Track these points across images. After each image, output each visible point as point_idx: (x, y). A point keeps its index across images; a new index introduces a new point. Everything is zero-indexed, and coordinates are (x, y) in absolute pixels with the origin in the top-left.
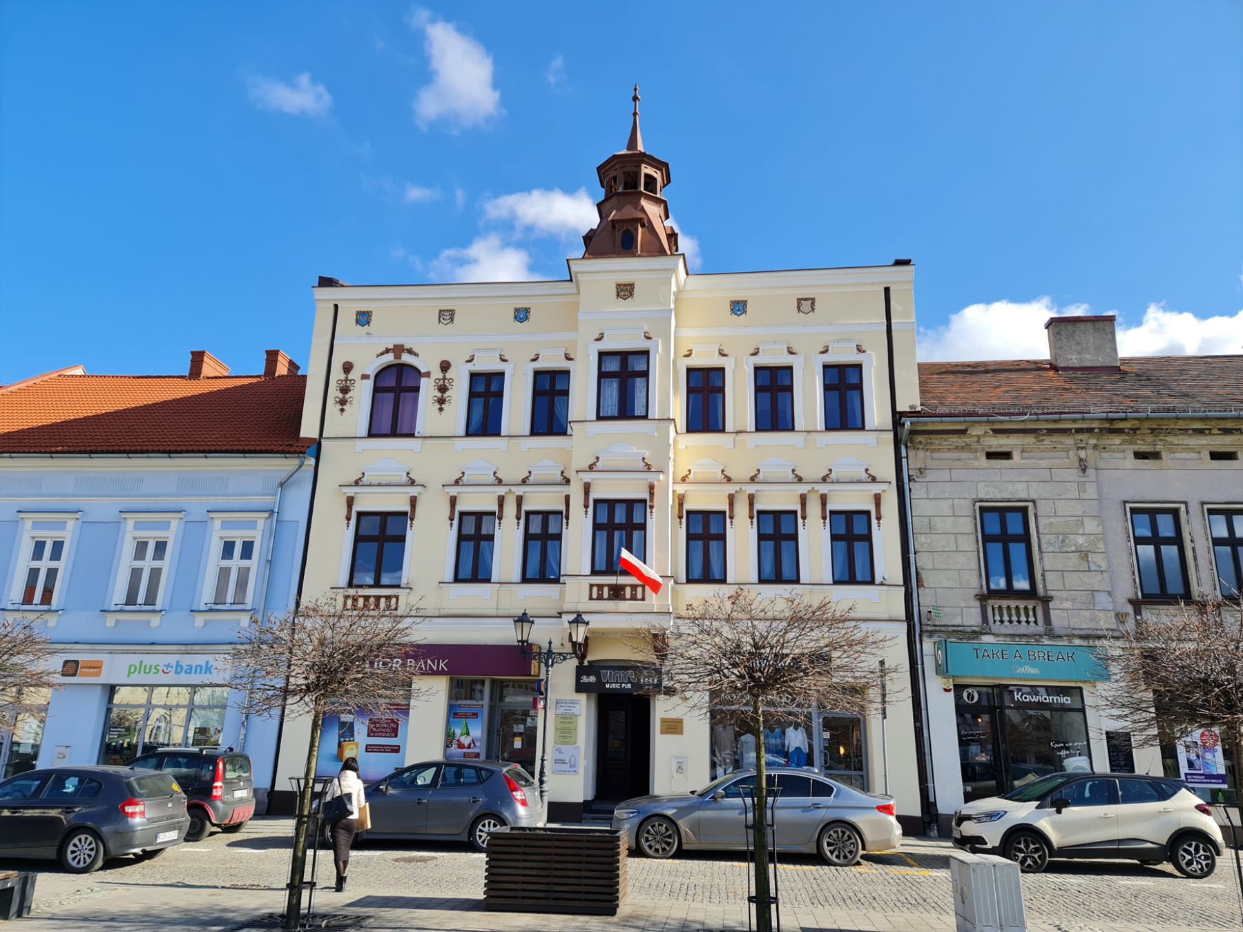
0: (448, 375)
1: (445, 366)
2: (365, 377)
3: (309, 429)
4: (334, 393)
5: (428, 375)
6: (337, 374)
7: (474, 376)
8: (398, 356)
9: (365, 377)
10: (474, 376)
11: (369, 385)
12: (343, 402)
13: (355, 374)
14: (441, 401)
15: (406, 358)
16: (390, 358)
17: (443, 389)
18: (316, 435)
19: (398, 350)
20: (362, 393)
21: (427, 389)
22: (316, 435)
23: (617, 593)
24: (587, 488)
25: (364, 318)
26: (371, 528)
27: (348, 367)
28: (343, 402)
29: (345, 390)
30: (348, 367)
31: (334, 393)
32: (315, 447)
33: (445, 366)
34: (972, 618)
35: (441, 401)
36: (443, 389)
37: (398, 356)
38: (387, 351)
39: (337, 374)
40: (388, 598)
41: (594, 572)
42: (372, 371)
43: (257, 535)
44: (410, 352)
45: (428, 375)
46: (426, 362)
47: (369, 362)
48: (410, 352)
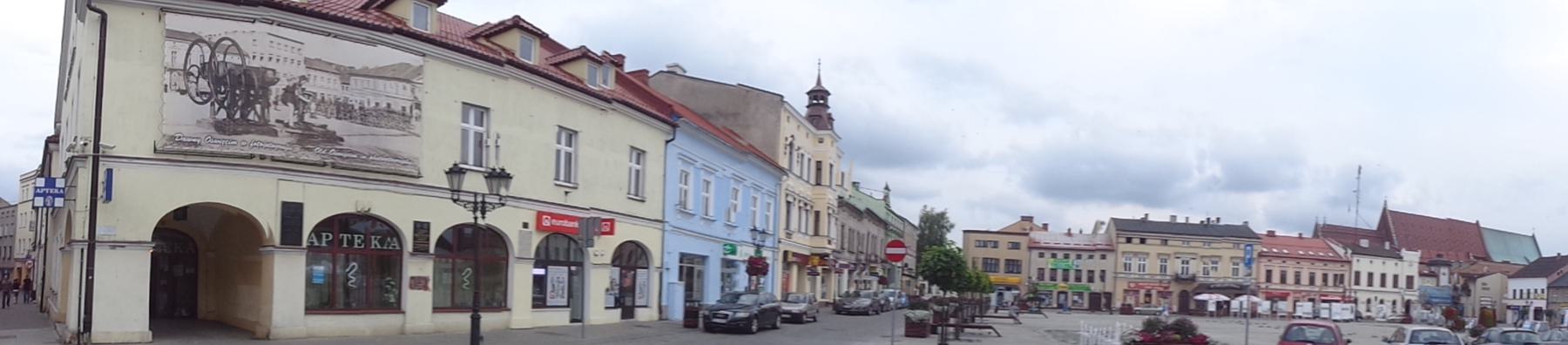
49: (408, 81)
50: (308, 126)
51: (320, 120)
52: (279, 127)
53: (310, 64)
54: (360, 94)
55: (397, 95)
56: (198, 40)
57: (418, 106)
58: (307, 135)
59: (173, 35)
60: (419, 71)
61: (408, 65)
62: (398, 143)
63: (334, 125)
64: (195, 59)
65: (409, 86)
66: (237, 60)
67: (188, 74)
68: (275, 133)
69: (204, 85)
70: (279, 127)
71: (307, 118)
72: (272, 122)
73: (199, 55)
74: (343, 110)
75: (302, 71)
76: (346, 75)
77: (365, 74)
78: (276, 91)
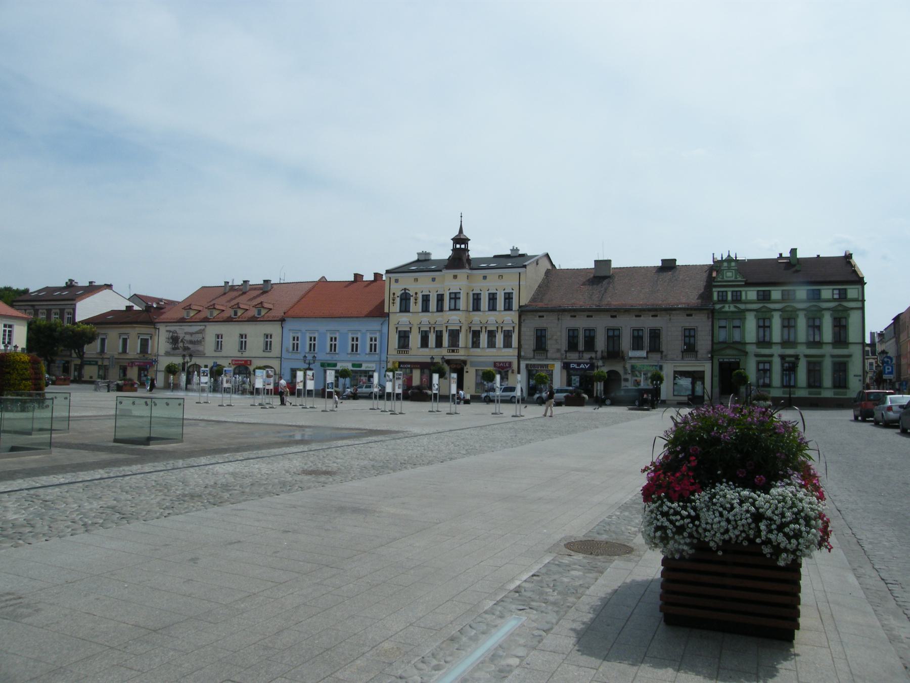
0: (417, 296)
1: (416, 294)
2: (398, 297)
3: (386, 310)
4: (391, 301)
5: (412, 296)
6: (392, 296)
7: (423, 296)
8: (405, 291)
9: (398, 297)
10: (423, 296)
11: (399, 299)
12: (393, 303)
13: (396, 296)
14: (416, 303)
15: (407, 291)
16: (403, 291)
17: (416, 300)
18: (388, 312)
19: (405, 289)
20: (398, 300)
21: (412, 300)
22: (388, 312)
23: (453, 351)
24: (447, 327)
25: (397, 281)
26: (402, 335)
27: (394, 294)
28: (393, 303)
29: (394, 300)
30: (394, 294)
31: (391, 301)
32: (388, 315)
33: (416, 294)
34: (532, 355)
35: (416, 303)
36: (416, 300)
37: (405, 291)
38: (403, 290)
39: (392, 296)
40: (407, 351)
41: (448, 347)
42: (399, 295)
43: (378, 336)
44: (408, 290)
45: (412, 296)
46: (412, 293)
47: (399, 293)
48: (408, 290)
49: (201, 333)
51: (187, 345)
53: (186, 333)
55: (198, 337)
57: (203, 338)
59: (167, 331)
60: (204, 330)
62: (200, 348)
63: (190, 346)
64: (170, 336)
66: (176, 335)
69: (171, 341)
71: (185, 345)
72: (179, 346)
73: (171, 334)
74: (191, 342)
75: (184, 335)
76: (191, 334)
78: (180, 340)
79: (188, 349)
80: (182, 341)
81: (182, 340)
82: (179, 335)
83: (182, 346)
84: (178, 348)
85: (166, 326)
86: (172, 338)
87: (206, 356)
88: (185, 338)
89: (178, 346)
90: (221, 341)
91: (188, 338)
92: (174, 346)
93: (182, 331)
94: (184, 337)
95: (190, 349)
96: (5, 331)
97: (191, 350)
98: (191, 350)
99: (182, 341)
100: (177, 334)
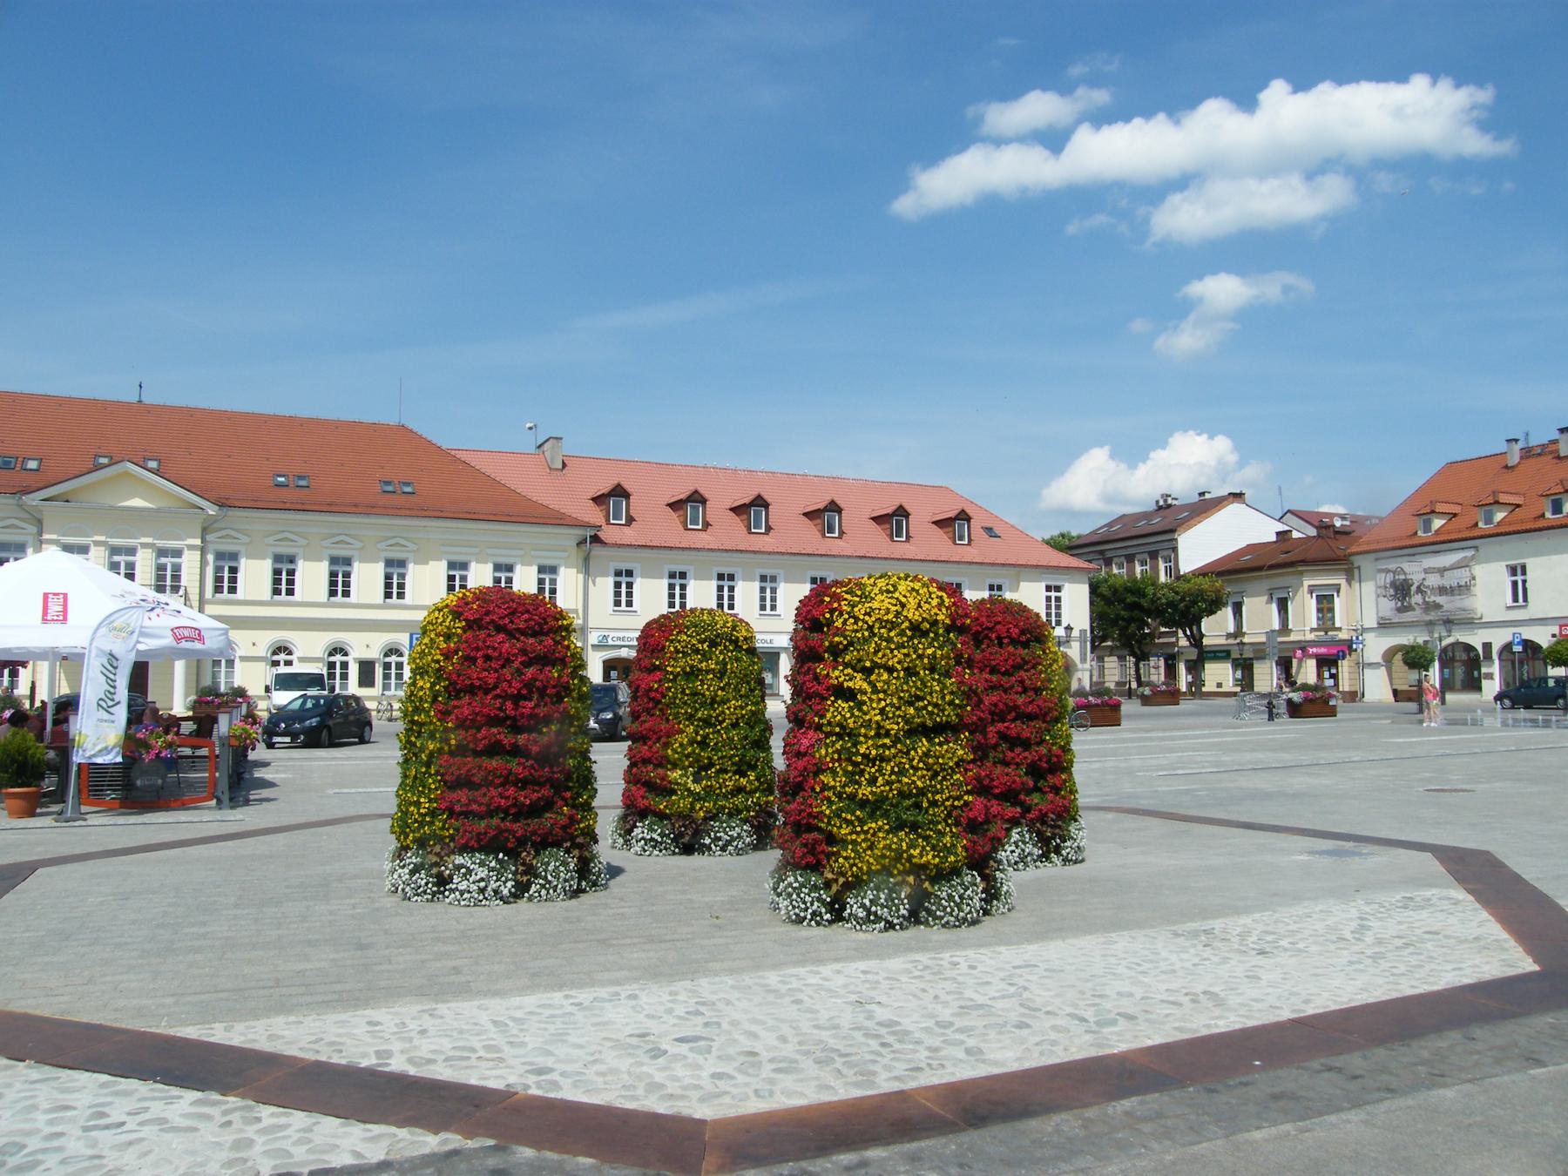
49: (1467, 566)
50: (1427, 603)
52: (1416, 606)
53: (1426, 571)
54: (1450, 580)
55: (1460, 576)
56: (1388, 571)
57: (1474, 578)
58: (1430, 607)
61: (1466, 557)
63: (1440, 600)
64: (1388, 581)
65: (1467, 569)
66: (1402, 577)
67: (1386, 587)
68: (1414, 609)
69: (1392, 592)
70: (1416, 606)
71: (1427, 599)
72: (1413, 603)
73: (1390, 577)
74: (1442, 590)
75: (1423, 576)
76: (1442, 571)
77: (1452, 568)
78: (1413, 588)
79: (1438, 606)
80: (1419, 590)
81: (1419, 587)
82: (1408, 577)
83: (1420, 601)
84: (1409, 608)
85: (1377, 559)
86: (1393, 584)
87: (1483, 620)
88: (1426, 583)
89: (1409, 603)
90: (1524, 582)
91: (1433, 580)
92: (1399, 604)
93: (1415, 569)
94: (1424, 579)
95: (1442, 606)
96: (1048, 599)
97: (1445, 609)
98: (1445, 609)
99: (1419, 590)
100: (1405, 574)
